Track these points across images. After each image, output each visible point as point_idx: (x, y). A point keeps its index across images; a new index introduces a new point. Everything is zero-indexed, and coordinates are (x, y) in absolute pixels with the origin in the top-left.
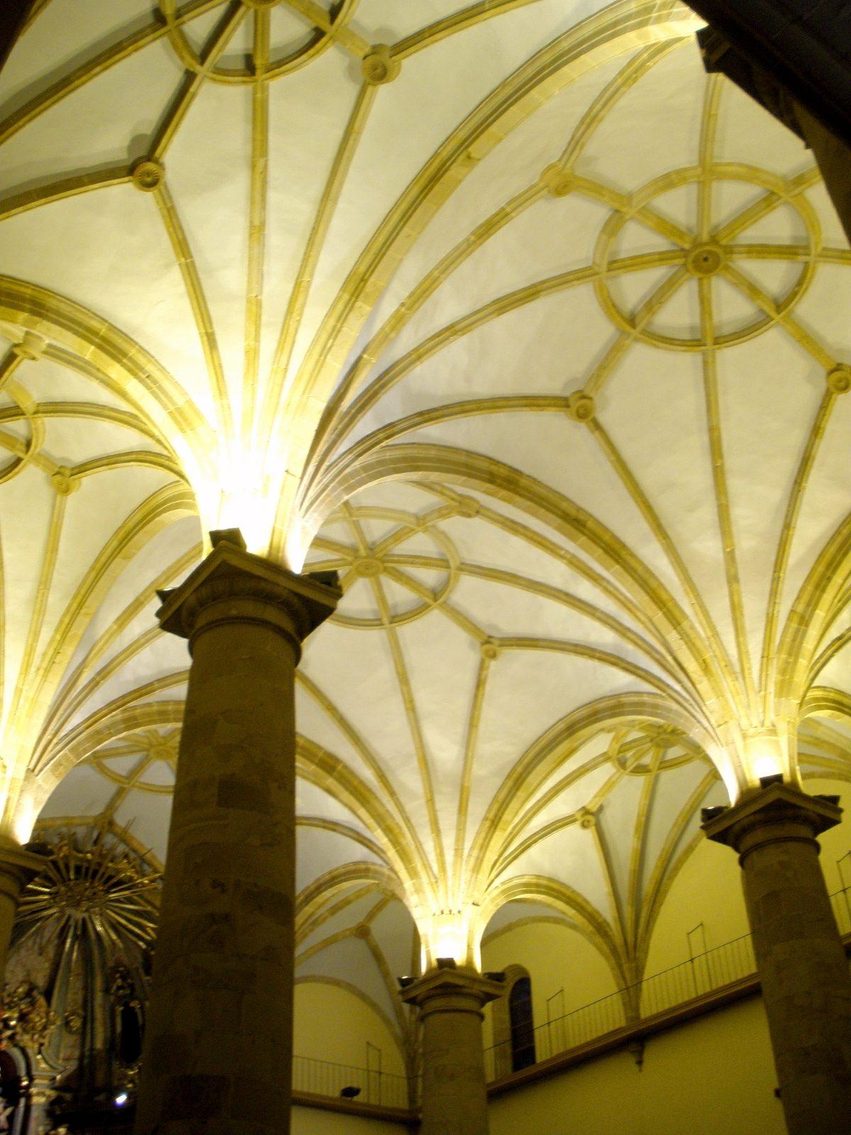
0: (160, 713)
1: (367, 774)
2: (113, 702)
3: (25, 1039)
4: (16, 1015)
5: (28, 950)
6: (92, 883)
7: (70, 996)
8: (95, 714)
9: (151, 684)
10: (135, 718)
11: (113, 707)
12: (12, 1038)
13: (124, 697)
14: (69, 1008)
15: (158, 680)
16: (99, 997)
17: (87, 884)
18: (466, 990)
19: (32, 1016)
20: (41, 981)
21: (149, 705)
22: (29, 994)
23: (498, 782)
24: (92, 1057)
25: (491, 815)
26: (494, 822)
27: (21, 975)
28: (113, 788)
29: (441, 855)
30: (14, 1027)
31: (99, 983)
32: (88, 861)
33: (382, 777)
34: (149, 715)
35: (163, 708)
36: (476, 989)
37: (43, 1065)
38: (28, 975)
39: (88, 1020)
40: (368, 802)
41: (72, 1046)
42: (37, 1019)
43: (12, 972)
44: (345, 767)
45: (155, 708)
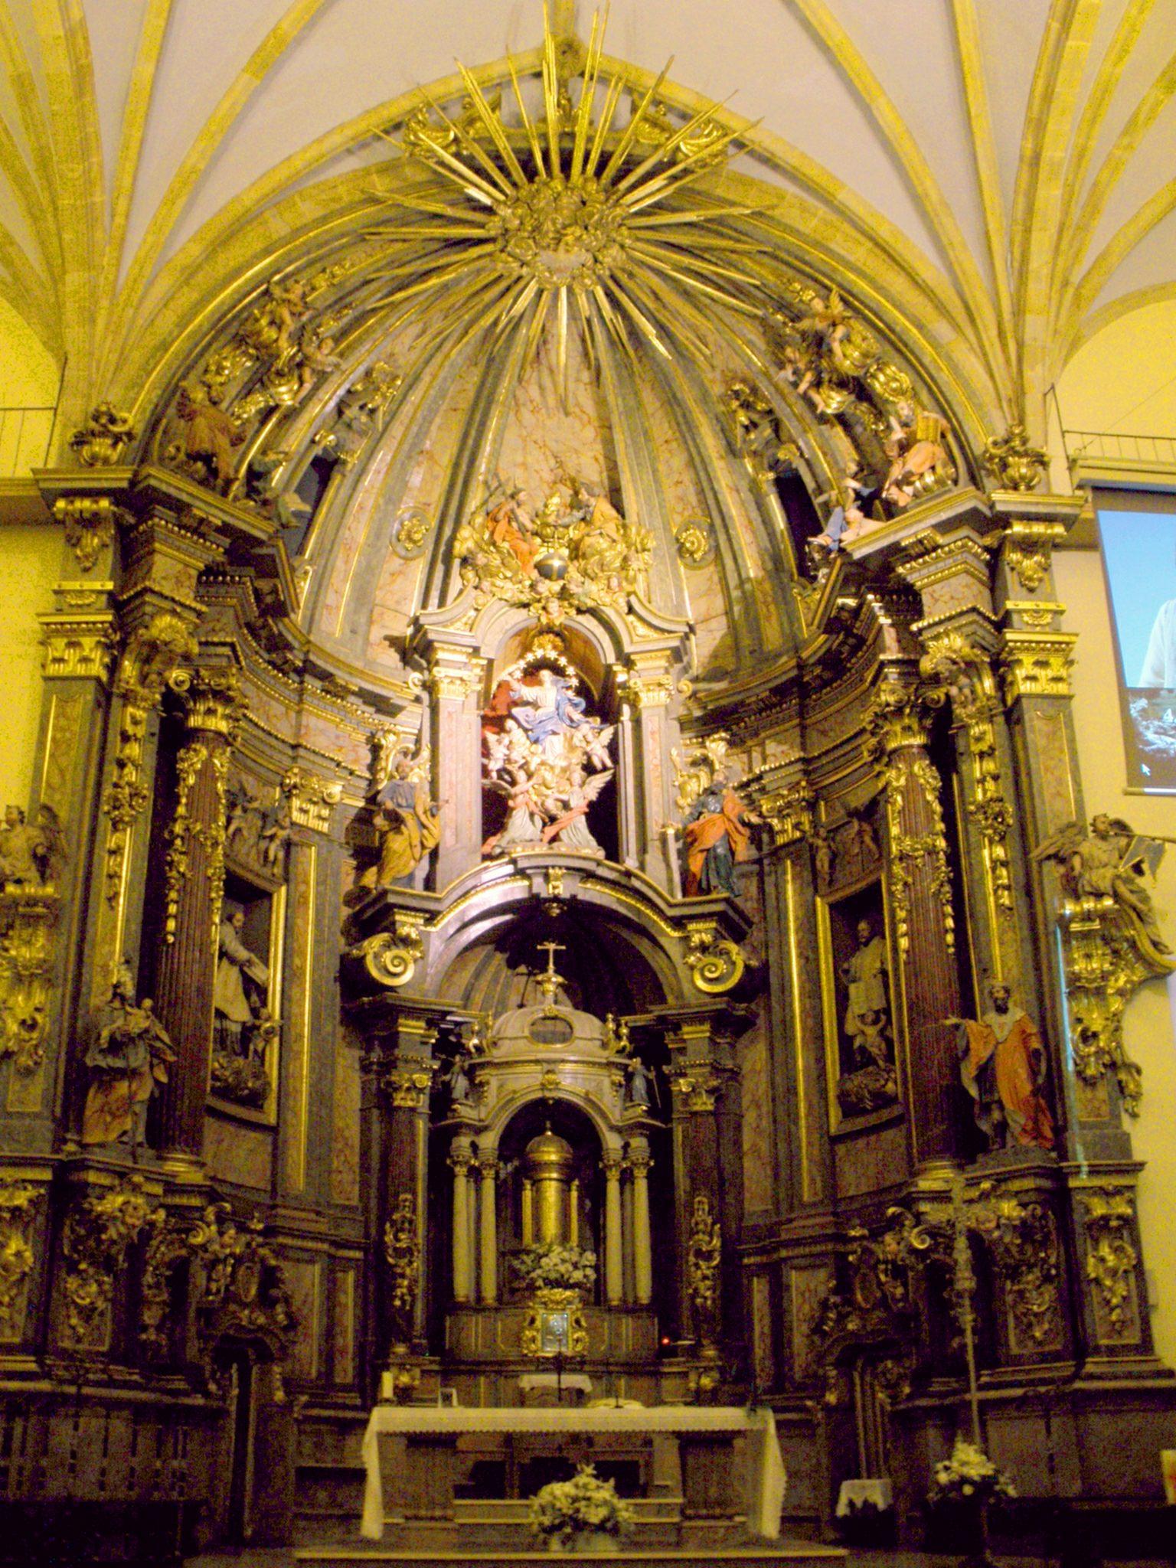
3: (593, 592)
4: (565, 552)
5: (535, 411)
7: (670, 493)
12: (564, 594)
14: (678, 519)
19: (588, 541)
20: (593, 472)
22: (576, 504)
24: (748, 600)
27: (545, 469)
31: (711, 443)
37: (642, 629)
38: (561, 464)
39: (716, 522)
41: (708, 592)
42: (603, 542)
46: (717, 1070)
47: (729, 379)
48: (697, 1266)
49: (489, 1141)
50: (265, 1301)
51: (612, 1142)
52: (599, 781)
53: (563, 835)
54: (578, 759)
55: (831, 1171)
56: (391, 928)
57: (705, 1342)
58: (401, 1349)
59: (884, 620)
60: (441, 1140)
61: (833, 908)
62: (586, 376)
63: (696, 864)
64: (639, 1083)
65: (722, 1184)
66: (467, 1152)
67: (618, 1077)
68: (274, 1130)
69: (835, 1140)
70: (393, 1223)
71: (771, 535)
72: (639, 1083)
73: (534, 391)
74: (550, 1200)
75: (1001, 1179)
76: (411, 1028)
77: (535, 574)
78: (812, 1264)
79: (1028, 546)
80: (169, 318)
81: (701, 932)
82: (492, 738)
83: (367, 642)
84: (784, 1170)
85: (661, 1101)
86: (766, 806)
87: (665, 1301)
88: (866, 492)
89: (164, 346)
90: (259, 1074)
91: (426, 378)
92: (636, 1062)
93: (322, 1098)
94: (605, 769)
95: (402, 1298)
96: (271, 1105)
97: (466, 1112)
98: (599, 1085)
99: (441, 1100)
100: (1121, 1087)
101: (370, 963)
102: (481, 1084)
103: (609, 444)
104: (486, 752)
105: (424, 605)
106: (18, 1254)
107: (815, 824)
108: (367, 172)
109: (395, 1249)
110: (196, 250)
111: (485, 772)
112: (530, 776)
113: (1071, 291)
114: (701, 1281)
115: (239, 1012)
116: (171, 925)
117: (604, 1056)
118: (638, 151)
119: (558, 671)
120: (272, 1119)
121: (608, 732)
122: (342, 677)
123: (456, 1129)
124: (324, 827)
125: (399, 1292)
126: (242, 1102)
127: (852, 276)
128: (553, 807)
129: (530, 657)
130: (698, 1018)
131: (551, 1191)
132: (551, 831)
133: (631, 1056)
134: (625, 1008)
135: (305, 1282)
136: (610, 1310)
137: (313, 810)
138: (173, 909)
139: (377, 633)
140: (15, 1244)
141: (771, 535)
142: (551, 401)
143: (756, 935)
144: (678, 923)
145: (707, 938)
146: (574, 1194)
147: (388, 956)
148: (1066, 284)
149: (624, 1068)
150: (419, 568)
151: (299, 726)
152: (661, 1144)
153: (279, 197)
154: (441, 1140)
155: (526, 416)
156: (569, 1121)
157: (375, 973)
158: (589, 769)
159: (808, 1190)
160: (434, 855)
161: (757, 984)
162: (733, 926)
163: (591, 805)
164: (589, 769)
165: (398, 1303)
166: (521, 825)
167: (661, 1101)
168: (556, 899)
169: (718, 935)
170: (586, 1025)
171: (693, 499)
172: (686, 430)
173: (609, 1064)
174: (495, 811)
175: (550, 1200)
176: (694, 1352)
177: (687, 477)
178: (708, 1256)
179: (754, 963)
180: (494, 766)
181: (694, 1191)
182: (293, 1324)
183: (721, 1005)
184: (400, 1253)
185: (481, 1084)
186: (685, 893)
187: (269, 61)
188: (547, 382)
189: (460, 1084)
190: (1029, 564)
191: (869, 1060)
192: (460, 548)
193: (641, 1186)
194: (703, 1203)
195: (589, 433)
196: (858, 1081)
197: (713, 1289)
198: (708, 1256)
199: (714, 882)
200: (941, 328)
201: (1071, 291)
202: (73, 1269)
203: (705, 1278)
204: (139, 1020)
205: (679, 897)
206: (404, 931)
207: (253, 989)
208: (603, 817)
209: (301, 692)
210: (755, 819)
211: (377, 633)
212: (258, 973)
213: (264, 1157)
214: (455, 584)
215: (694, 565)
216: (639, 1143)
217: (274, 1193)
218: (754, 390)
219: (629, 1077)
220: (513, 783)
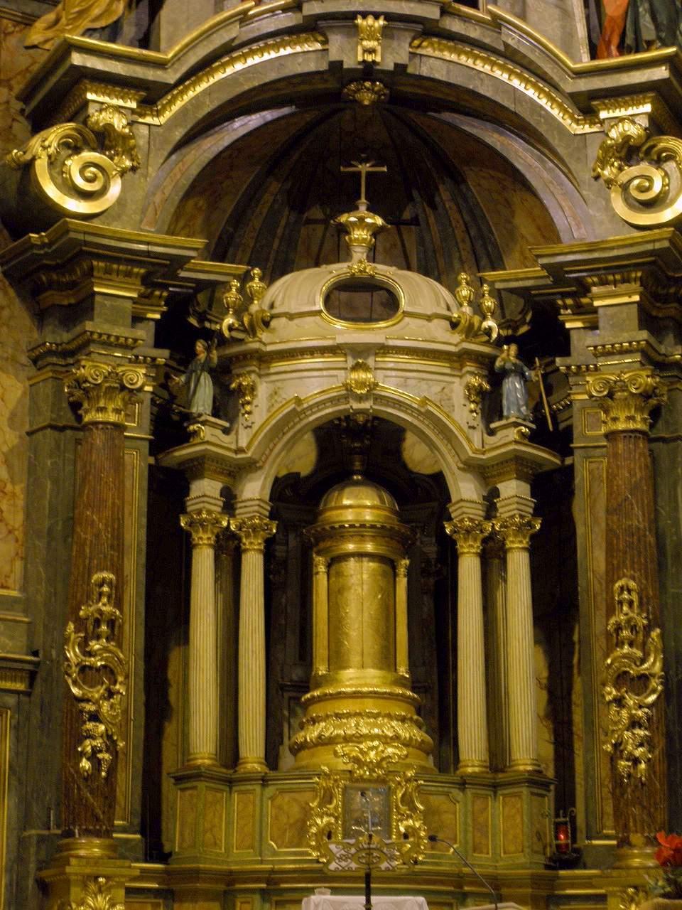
48: (619, 702)
49: (255, 490)
51: (465, 490)
56: (80, 112)
57: (636, 838)
58: (90, 848)
60: (168, 489)
64: (513, 388)
70: (81, 624)
74: (358, 596)
76: (116, 292)
95: (93, 757)
97: (209, 437)
99: (170, 425)
101: (41, 166)
102: (240, 391)
109: (83, 669)
117: (452, 341)
123: (195, 468)
125: (88, 746)
131: (360, 577)
134: (487, 255)
136: (463, 784)
144: (586, 106)
146: (402, 583)
149: (486, 364)
152: (553, 492)
154: (168, 489)
157: (52, 191)
165: (85, 764)
168: (368, 71)
173: (457, 359)
175: (358, 596)
178: (642, 681)
185: (240, 391)
186: (594, 55)
189: (204, 396)
193: (519, 564)
197: (645, 742)
203: (634, 723)
205: (586, 62)
206: (99, 118)
216: (513, 490)
219: (497, 378)
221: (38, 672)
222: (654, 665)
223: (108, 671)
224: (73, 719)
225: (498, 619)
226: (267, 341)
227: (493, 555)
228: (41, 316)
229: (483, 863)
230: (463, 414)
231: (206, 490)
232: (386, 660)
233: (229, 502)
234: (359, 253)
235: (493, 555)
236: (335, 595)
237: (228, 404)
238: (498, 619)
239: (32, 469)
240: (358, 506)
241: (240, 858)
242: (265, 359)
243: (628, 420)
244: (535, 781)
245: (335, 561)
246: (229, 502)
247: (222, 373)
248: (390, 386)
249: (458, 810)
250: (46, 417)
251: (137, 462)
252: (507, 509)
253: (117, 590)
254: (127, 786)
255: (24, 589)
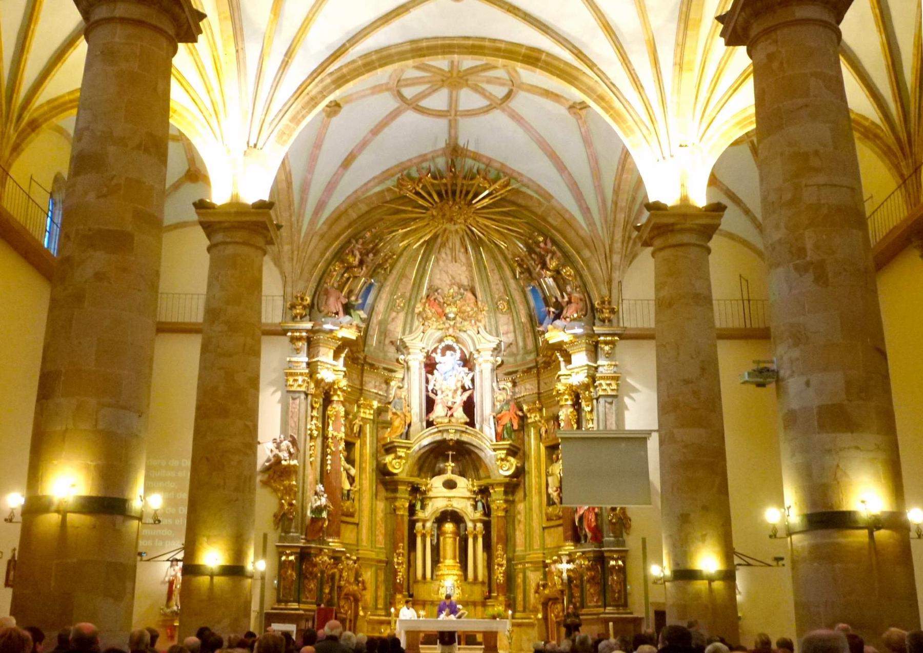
0: (365, 65)
1: (566, 55)
2: (315, 71)
6: (454, 200)
8: (301, 85)
9: (344, 45)
10: (344, 76)
11: (315, 75)
12: (454, 326)
13: (322, 64)
14: (497, 296)
15: (348, 41)
16: (512, 283)
17: (451, 203)
18: (679, 226)
21: (353, 61)
23: (674, 26)
25: (678, 61)
26: (680, 65)
28: (443, 123)
29: (647, 106)
30: (454, 319)
32: (446, 185)
33: (579, 54)
34: (355, 70)
35: (368, 60)
36: (689, 224)
37: (483, 340)
38: (453, 278)
40: (576, 79)
41: (507, 324)
43: (440, 279)
44: (548, 55)
45: (360, 63)
46: (506, 501)
47: (514, 256)
49: (428, 525)
50: (357, 581)
51: (470, 525)
52: (467, 394)
53: (455, 415)
54: (459, 385)
55: (543, 538)
56: (395, 452)
58: (399, 596)
59: (561, 359)
60: (412, 524)
61: (547, 448)
62: (462, 250)
63: (500, 429)
64: (480, 505)
65: (508, 541)
66: (421, 528)
67: (472, 502)
68: (357, 524)
69: (544, 528)
71: (529, 308)
72: (480, 505)
73: (444, 255)
74: (449, 545)
75: (583, 553)
77: (444, 318)
78: (536, 570)
79: (606, 343)
80: (317, 254)
81: (502, 454)
82: (430, 376)
83: (384, 344)
84: (529, 535)
85: (487, 511)
86: (525, 408)
87: (489, 582)
88: (557, 312)
89: (316, 265)
90: (353, 507)
91: (405, 254)
92: (479, 497)
93: (372, 512)
94: (469, 389)
96: (356, 515)
97: (420, 514)
98: (466, 506)
99: (412, 510)
100: (624, 525)
103: (471, 271)
104: (427, 381)
105: (404, 333)
106: (291, 575)
107: (541, 417)
108: (383, 191)
110: (325, 228)
111: (427, 391)
112: (442, 392)
113: (631, 242)
114: (499, 575)
115: (347, 486)
116: (329, 467)
117: (468, 494)
118: (479, 190)
119: (454, 350)
120: (357, 521)
121: (471, 375)
122: (377, 364)
123: (417, 521)
124: (372, 417)
126: (347, 516)
127: (554, 232)
128: (450, 404)
129: (443, 344)
130: (499, 484)
132: (450, 413)
133: (477, 494)
135: (368, 575)
137: (368, 411)
138: (329, 462)
139: (387, 341)
140: (289, 572)
141: (529, 308)
142: (450, 258)
143: (521, 453)
145: (503, 456)
147: (394, 461)
148: (630, 238)
149: (474, 499)
150: (402, 316)
151: (362, 381)
152: (487, 525)
153: (353, 205)
155: (441, 263)
156: (455, 517)
157: (391, 469)
158: (464, 389)
159: (537, 544)
160: (409, 425)
161: (520, 473)
162: (513, 452)
163: (465, 403)
164: (464, 389)
166: (439, 411)
167: (487, 511)
169: (507, 454)
170: (462, 482)
171: (502, 289)
172: (499, 267)
173: (469, 498)
174: (430, 404)
176: (496, 598)
177: (500, 283)
178: (502, 566)
179: (519, 465)
180: (430, 387)
181: (497, 543)
182: (364, 589)
183: (507, 480)
184: (398, 564)
187: (347, 163)
188: (449, 252)
189: (418, 506)
190: (607, 348)
191: (554, 503)
192: (417, 311)
194: (500, 547)
195: (464, 268)
196: (550, 509)
198: (502, 566)
199: (506, 436)
200: (587, 253)
201: (631, 242)
202: (306, 577)
204: (323, 501)
206: (400, 454)
207: (352, 480)
208: (469, 407)
209: (362, 371)
210: (520, 414)
211: (387, 341)
212: (353, 472)
213: (354, 533)
214: (416, 323)
215: (502, 313)
217: (357, 545)
218: (522, 260)
219: (476, 502)
220: (436, 394)
221: (389, 563)
222: (504, 562)
223: (402, 563)
224: (395, 573)
225: (476, 550)
226: (431, 494)
227: (475, 538)
228: (387, 490)
229: (473, 598)
230: (470, 509)
231: (419, 525)
232: (454, 558)
233: (424, 526)
234: (449, 472)
235: (475, 538)
236: (444, 545)
237: (423, 507)
238: (476, 550)
239: (386, 521)
240: (449, 527)
241: (426, 597)
242: (431, 498)
243: (501, 514)
244: (483, 583)
245: (444, 539)
246: (424, 526)
247: (422, 501)
248: (455, 505)
249: (467, 588)
250: (388, 511)
251: (406, 519)
252: (478, 529)
253: (403, 547)
254: (405, 585)
255: (385, 544)
